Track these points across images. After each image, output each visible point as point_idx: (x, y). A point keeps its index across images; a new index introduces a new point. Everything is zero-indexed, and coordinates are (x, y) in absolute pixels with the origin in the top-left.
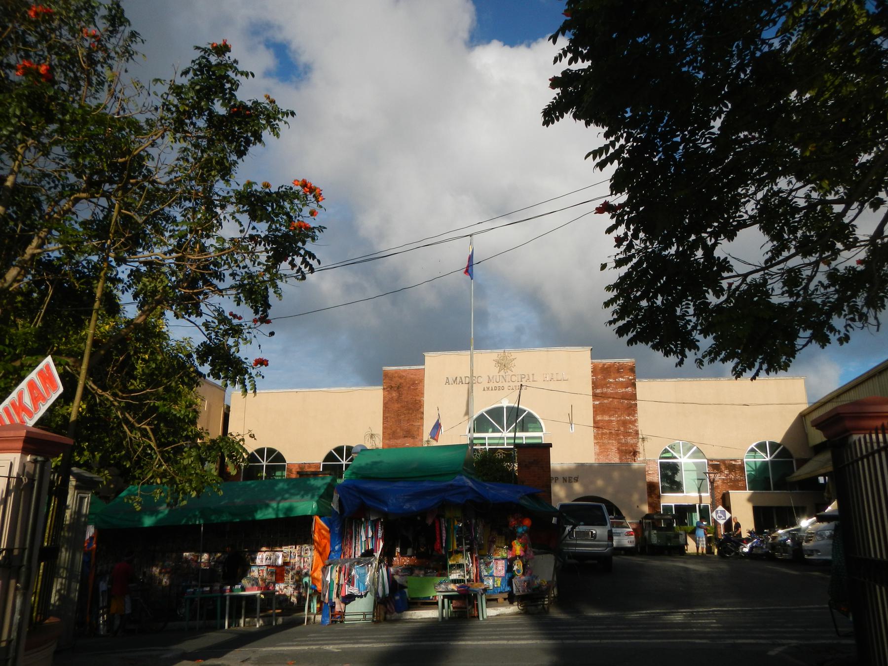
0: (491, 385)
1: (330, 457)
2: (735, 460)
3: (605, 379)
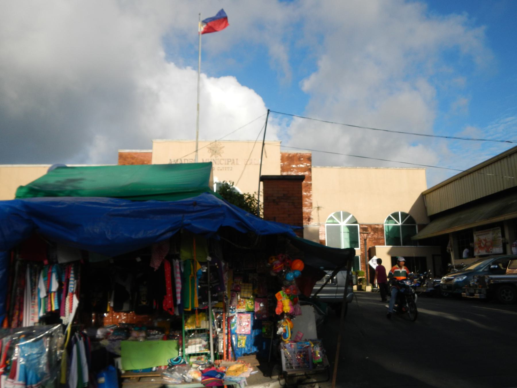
2: (378, 225)
3: (290, 165)
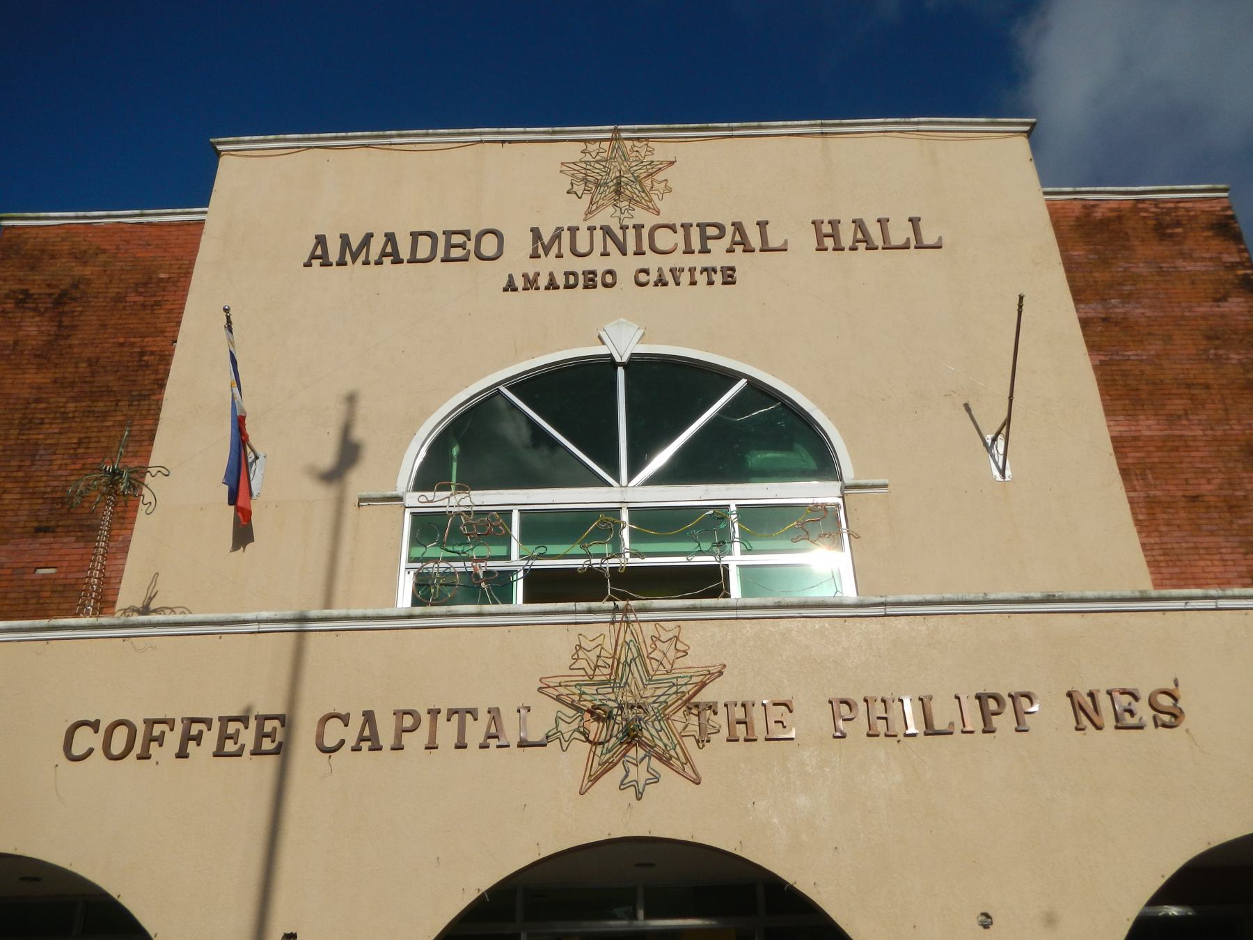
0: (548, 265)
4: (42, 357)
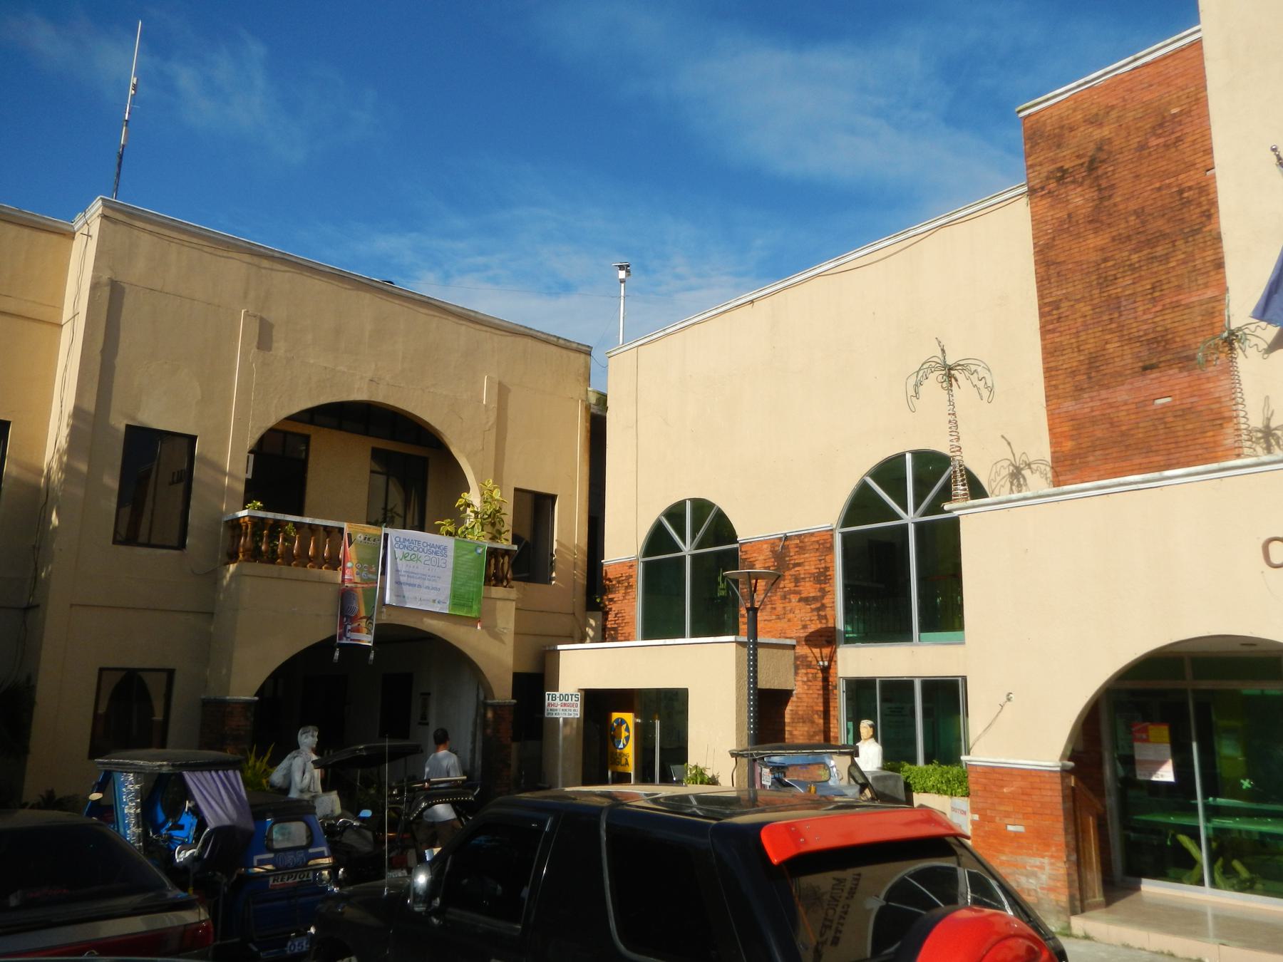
1: (862, 505)
4: (1095, 221)
